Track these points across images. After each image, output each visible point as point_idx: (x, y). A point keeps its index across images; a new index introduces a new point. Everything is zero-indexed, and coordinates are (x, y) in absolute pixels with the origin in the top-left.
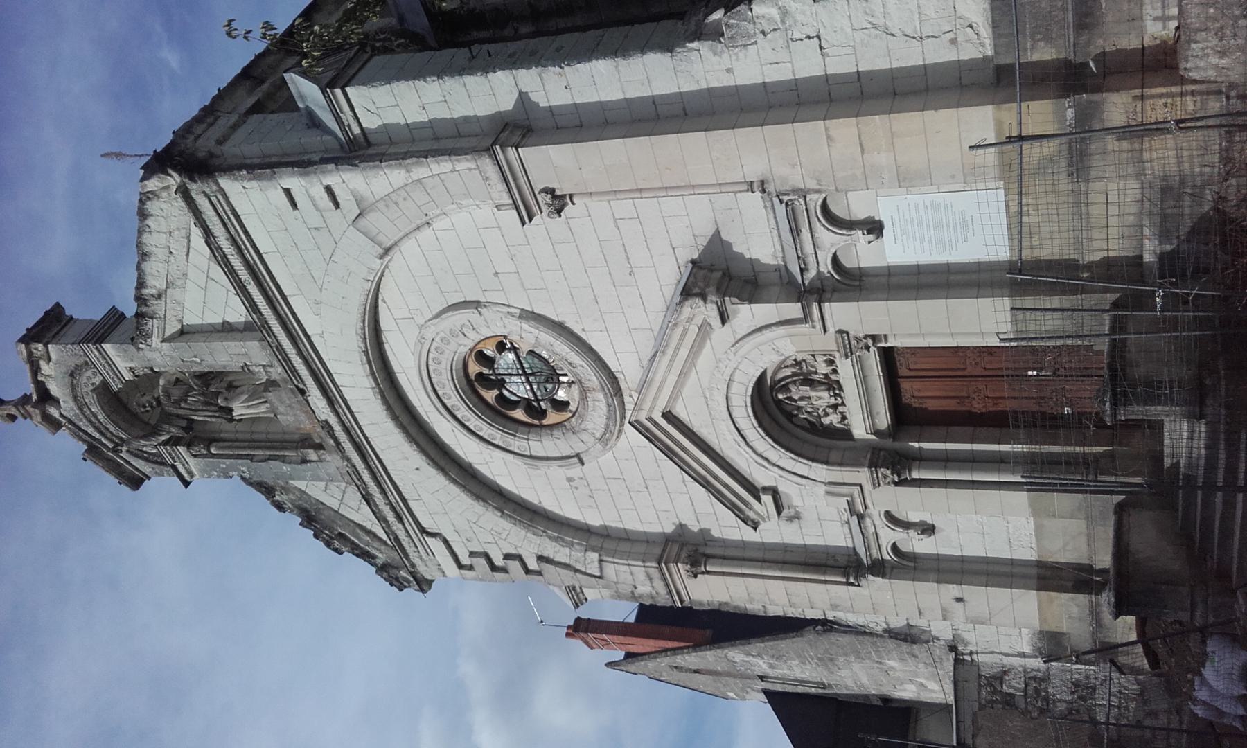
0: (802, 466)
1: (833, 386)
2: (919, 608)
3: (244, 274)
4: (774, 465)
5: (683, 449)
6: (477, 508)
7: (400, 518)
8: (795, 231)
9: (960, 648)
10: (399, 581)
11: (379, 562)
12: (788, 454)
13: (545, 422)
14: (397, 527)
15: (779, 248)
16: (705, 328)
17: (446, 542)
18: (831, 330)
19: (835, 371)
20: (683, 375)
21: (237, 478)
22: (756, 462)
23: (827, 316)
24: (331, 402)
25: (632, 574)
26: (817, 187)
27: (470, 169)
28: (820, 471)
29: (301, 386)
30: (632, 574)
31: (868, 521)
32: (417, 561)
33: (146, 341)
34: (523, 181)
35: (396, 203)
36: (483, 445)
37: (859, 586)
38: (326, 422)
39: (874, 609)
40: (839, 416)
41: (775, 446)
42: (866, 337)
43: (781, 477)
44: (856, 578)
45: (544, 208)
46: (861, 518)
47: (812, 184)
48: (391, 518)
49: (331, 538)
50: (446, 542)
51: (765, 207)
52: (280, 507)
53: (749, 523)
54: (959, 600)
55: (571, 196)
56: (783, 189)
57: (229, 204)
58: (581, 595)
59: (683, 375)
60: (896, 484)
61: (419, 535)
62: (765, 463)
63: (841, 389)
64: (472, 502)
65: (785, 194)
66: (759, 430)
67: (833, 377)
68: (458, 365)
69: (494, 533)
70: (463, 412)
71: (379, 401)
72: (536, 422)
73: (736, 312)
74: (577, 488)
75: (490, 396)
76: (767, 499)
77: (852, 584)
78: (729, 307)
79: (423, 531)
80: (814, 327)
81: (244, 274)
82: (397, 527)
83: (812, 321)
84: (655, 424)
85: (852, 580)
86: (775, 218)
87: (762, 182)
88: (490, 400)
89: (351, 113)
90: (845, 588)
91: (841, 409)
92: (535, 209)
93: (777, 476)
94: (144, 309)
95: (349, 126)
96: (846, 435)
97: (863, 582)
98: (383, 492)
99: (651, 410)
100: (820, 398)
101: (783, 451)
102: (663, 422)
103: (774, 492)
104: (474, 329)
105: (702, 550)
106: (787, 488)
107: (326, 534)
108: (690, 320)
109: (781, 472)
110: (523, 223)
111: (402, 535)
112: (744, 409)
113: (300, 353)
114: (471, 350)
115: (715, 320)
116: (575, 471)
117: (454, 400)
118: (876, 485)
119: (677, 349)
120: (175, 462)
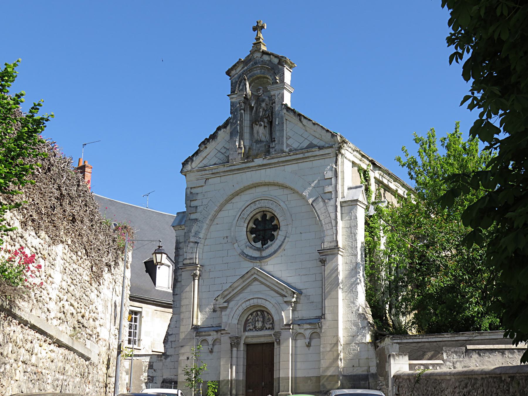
0: (237, 317)
1: (261, 329)
5: (244, 282)
9: (163, 357)
13: (248, 233)
18: (282, 331)
19: (266, 329)
20: (268, 287)
21: (230, 116)
23: (286, 330)
24: (260, 166)
26: (322, 331)
31: (215, 333)
35: (325, 212)
40: (252, 329)
42: (280, 340)
45: (321, 257)
47: (323, 331)
54: (188, 358)
55: (324, 265)
56: (322, 323)
57: (328, 158)
59: (268, 287)
63: (260, 330)
67: (265, 328)
70: (253, 207)
74: (224, 239)
76: (225, 305)
84: (252, 275)
88: (256, 216)
91: (254, 329)
92: (321, 255)
96: (245, 330)
97: (193, 330)
99: (257, 274)
100: (258, 324)
102: (253, 277)
110: (318, 251)
111: (207, 172)
114: (275, 215)
117: (258, 205)
118: (230, 338)
119: (278, 287)
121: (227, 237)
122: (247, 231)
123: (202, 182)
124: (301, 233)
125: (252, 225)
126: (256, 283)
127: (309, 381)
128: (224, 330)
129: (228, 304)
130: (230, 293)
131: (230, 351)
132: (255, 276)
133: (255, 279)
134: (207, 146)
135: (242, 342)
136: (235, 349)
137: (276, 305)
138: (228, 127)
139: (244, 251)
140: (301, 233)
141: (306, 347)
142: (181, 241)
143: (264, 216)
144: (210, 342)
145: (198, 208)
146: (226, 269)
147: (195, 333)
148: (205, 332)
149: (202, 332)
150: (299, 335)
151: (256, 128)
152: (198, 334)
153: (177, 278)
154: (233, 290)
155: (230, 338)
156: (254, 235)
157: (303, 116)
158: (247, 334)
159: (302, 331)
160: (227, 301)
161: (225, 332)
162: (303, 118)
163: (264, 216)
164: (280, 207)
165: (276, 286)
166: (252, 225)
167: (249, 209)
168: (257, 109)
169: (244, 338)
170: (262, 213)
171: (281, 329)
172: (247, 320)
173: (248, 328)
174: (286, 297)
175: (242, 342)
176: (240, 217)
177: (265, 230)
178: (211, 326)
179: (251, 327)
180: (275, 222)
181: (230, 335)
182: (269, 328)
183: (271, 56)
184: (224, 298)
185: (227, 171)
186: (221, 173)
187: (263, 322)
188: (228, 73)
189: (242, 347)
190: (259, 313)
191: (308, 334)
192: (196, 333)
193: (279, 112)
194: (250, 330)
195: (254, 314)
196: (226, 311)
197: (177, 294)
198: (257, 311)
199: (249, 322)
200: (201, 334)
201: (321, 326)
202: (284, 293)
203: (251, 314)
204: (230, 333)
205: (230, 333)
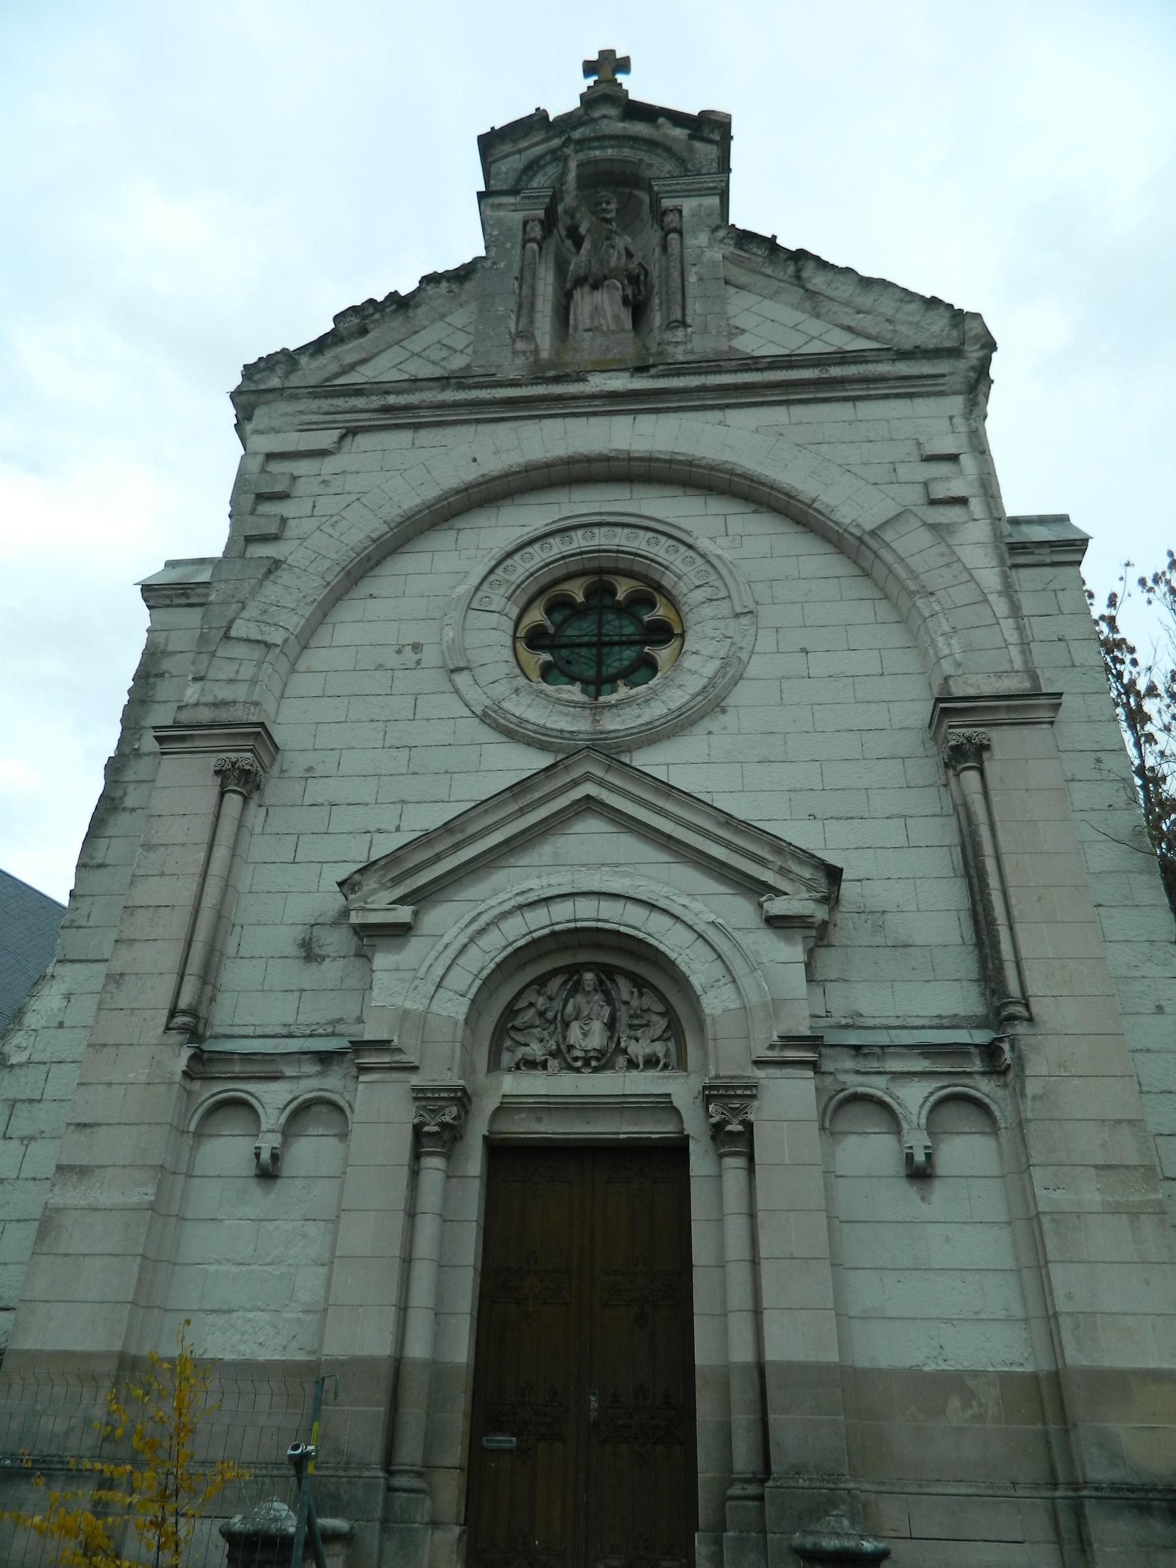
1: (600, 1061)
2: (98, 1125)
3: (835, 372)
4: (472, 940)
5: (522, 812)
6: (393, 513)
7: (386, 409)
8: (928, 1050)
10: (265, 369)
11: (304, 360)
12: (492, 965)
13: (521, 646)
14: (376, 402)
15: (870, 1022)
16: (756, 889)
17: (323, 453)
18: (760, 1073)
19: (632, 1064)
22: (480, 914)
25: (231, 681)
27: (1011, 661)
28: (458, 1009)
29: (653, 371)
30: (231, 681)
31: (311, 1068)
32: (301, 405)
33: (732, 238)
34: (1002, 716)
36: (497, 553)
37: (168, 1028)
38: (584, 380)
39: (105, 1045)
40: (540, 1059)
41: (510, 949)
42: (749, 1126)
43: (447, 946)
44: (183, 1029)
46: (325, 1058)
48: (392, 400)
49: (365, 317)
50: (323, 453)
51: (940, 1017)
52: (430, 280)
53: (357, 877)
58: (167, 602)
59: (666, 842)
60: (417, 1130)
61: (347, 425)
62: (481, 922)
63: (596, 1070)
64: (405, 506)
65: (1012, 1047)
66: (546, 931)
67: (621, 1061)
68: (639, 566)
69: (334, 519)
70: (557, 547)
71: (606, 452)
72: (521, 633)
73: (789, 940)
74: (399, 652)
75: (577, 591)
76: (404, 914)
77: (173, 1014)
78: (798, 935)
79: (352, 432)
80: (771, 1047)
81: (835, 372)
82: (376, 402)
83: (783, 1047)
84: (575, 783)
85: (180, 1020)
86: (923, 1027)
87: (1030, 1020)
89: (1048, 560)
90: (165, 1004)
91: (553, 1063)
93: (446, 939)
94: (783, 256)
95: (1032, 553)
96: (494, 1065)
97: (175, 1037)
98: (443, 406)
99: (601, 783)
101: (498, 959)
102: (577, 793)
103: (402, 931)
104: (711, 600)
105: (256, 796)
106: (413, 951)
107: (372, 314)
108: (783, 872)
109: (456, 946)
111: (360, 402)
112: (594, 915)
113: (703, 389)
115: (777, 907)
116: (430, 655)
118: (420, 1095)
119: (728, 845)
120: (524, 198)
121: (417, 647)
122: (515, 638)
123: (325, 439)
124: (804, 651)
125: (536, 615)
126: (591, 825)
127: (955, 1403)
128: (382, 1045)
129: (416, 914)
130: (438, 858)
131: (405, 1172)
132: (590, 789)
133: (589, 805)
134: (370, 327)
135: (478, 1128)
136: (433, 1164)
137: (712, 935)
138: (469, 285)
139: (505, 705)
140: (804, 651)
141: (904, 1184)
142: (170, 648)
143: (600, 591)
144: (272, 1117)
145: (292, 523)
146: (404, 770)
147: (186, 1053)
148: (248, 1057)
149: (227, 1057)
150: (856, 1110)
151: (584, 303)
152: (199, 1068)
153: (118, 794)
154: (457, 847)
155: (420, 1095)
156: (546, 657)
157: (817, 259)
158: (511, 1084)
159: (876, 1086)
160: (420, 898)
161: (386, 1059)
162: (811, 265)
163: (600, 591)
164: (690, 553)
165: (717, 839)
166: (536, 615)
167: (538, 556)
168: (596, 247)
169: (490, 1104)
170: (594, 578)
171: (759, 1063)
172: (510, 1012)
173: (506, 1059)
174: (779, 893)
175: (478, 1128)
176: (493, 577)
177: (601, 645)
178: (284, 1031)
179: (536, 1050)
180: (661, 611)
181: (415, 1080)
182: (651, 1062)
183: (661, 120)
184: (397, 881)
185: (456, 405)
186: (422, 412)
187: (611, 1026)
188: (489, 143)
189: (474, 1163)
190: (589, 977)
191: (915, 1109)
192: (192, 1058)
193: (702, 252)
194: (531, 1064)
195: (554, 985)
196: (399, 948)
197: (101, 866)
198: (573, 971)
199: (518, 1022)
200: (217, 1069)
201: (1020, 1060)
202: (768, 877)
203: (541, 982)
204: (414, 1069)
205: (414, 1069)
